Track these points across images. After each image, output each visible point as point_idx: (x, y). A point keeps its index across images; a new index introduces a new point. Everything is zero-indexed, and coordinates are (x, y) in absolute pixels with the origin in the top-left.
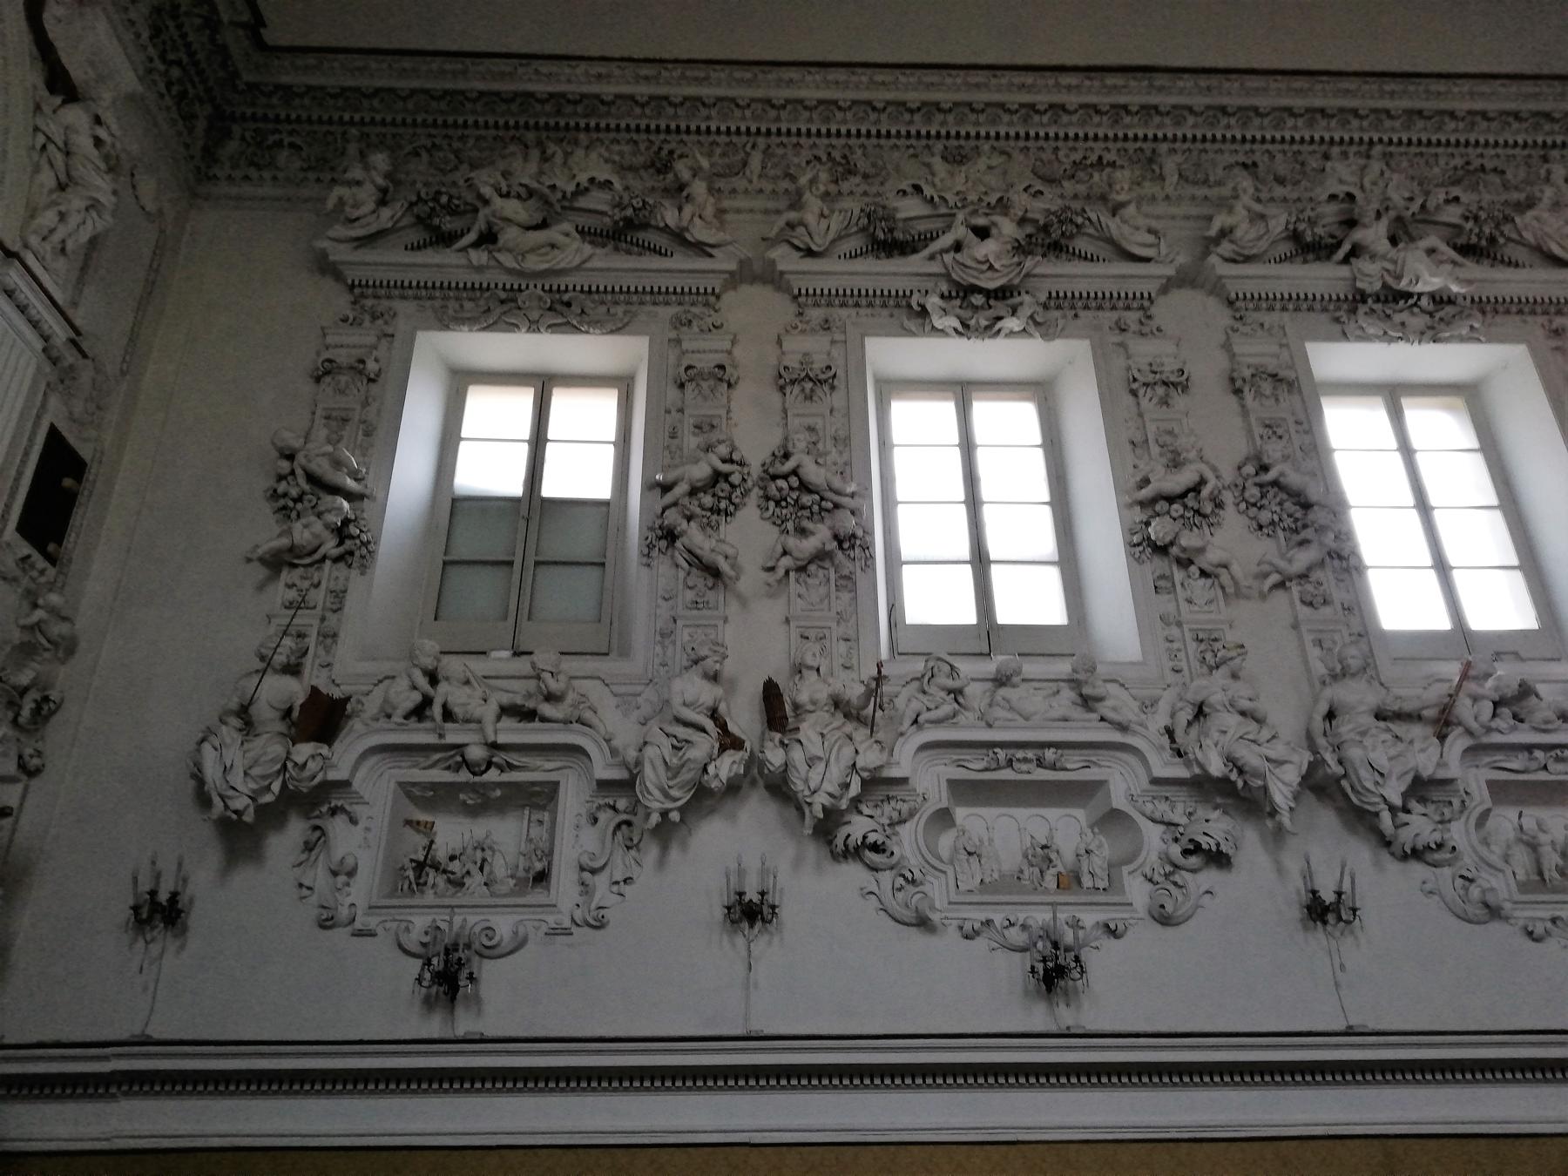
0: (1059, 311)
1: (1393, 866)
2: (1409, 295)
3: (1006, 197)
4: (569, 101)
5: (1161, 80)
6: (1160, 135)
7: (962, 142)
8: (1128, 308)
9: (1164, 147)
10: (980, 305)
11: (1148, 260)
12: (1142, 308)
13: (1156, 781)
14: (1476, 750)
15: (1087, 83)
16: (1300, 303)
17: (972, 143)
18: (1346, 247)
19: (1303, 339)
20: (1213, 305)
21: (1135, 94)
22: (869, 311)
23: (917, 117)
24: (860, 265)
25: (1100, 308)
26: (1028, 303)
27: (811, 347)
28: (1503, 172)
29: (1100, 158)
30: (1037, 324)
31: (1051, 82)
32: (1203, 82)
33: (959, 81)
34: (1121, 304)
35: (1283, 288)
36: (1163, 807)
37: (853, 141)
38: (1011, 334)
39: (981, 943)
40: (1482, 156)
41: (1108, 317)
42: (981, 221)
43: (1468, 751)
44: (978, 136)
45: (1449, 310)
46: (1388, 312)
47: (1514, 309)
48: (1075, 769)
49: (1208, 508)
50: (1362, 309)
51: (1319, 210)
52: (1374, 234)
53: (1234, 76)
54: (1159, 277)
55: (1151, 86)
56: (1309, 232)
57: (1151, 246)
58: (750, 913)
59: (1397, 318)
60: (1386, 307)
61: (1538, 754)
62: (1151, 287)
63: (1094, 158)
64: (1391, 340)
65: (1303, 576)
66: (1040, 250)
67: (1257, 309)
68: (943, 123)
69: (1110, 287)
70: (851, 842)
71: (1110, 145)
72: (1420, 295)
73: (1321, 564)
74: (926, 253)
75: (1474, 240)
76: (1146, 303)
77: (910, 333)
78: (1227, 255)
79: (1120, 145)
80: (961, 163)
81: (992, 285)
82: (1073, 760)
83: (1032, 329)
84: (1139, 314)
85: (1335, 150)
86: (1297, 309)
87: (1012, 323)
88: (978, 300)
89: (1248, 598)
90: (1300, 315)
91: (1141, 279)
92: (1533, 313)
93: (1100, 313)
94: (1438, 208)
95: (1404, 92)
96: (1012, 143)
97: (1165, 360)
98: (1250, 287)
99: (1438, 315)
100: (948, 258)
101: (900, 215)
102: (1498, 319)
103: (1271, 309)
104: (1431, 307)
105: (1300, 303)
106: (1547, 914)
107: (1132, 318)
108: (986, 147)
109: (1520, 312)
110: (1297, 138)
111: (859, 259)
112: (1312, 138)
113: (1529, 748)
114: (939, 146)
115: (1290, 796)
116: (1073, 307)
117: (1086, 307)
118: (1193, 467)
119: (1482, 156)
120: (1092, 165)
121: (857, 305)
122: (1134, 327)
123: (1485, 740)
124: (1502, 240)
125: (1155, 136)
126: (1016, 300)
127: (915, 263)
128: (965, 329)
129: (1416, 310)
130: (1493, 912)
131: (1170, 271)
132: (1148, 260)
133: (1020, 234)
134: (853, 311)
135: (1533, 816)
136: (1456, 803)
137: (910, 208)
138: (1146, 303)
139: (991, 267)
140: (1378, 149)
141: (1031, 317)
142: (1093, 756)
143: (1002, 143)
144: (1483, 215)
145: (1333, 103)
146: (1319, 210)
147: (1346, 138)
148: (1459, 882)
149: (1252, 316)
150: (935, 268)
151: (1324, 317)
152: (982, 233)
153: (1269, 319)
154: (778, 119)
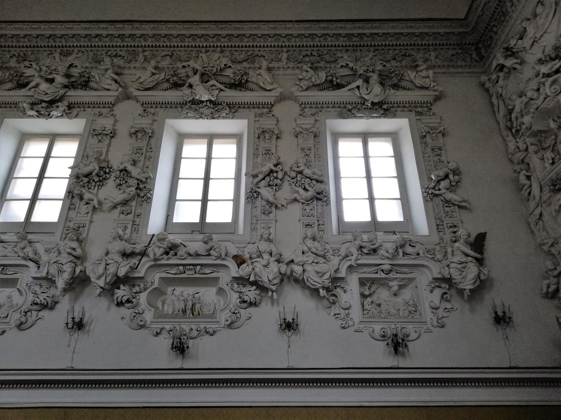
0: (71, 110)
1: (114, 308)
2: (202, 102)
3: (208, 67)
4: (150, 37)
5: (137, 25)
6: (140, 45)
7: (69, 49)
8: (104, 107)
9: (140, 49)
10: (45, 107)
11: (109, 90)
12: (109, 107)
13: (35, 278)
14: (156, 266)
15: (110, 27)
16: (166, 105)
17: (72, 49)
18: (187, 85)
19: (87, 119)
20: (138, 105)
21: (128, 30)
22: (10, 109)
23: (50, 40)
24: (13, 93)
25: (94, 107)
26: (62, 106)
27: (144, 122)
28: (264, 57)
29: (116, 54)
30: (66, 113)
31: (96, 26)
32: (152, 26)
33: (63, 27)
34: (101, 106)
35: (159, 100)
36: (37, 288)
37: (29, 49)
38: (57, 117)
39: (161, 337)
40: (259, 50)
41: (96, 110)
42: (50, 77)
43: (151, 267)
44: (73, 46)
45: (219, 106)
46: (197, 108)
47: (246, 106)
48: (10, 274)
49: (96, 179)
50: (187, 106)
51: (179, 71)
52: (195, 80)
53: (163, 23)
54: (114, 96)
55: (133, 27)
56: (171, 79)
57: (110, 85)
58: (79, 325)
59: (201, 110)
60: (194, 107)
61: (181, 268)
62: (112, 100)
63: (114, 54)
64: (197, 118)
65: (125, 203)
66: (80, 87)
67: (151, 107)
68: (295, 41)
69: (96, 100)
70: (119, 300)
71: (122, 49)
72: (207, 101)
73: (132, 199)
74: (28, 88)
75: (233, 81)
76: (111, 106)
77: (20, 117)
78: (136, 87)
79: (126, 49)
80: (67, 56)
81: (47, 99)
82: (10, 271)
83: (64, 114)
84: (109, 109)
85: (203, 50)
86: (166, 107)
87: (54, 113)
88: (44, 105)
89: (104, 211)
90: (167, 109)
91: (109, 96)
92: (254, 108)
93: (94, 109)
94: (221, 70)
95: (380, 26)
96: (87, 49)
97: (106, 126)
98: (148, 100)
99: (216, 109)
100: (33, 90)
101: (26, 75)
102: (240, 110)
103: (156, 107)
104: (212, 106)
105: (166, 105)
106: (161, 326)
107: (105, 111)
108: (76, 50)
109: (249, 108)
110: (190, 45)
111: (12, 91)
112: (195, 45)
113: (178, 265)
114: (59, 50)
115: (64, 284)
116: (84, 107)
117: (89, 107)
118: (92, 164)
119: (259, 50)
120: (114, 56)
121: (6, 107)
122: (104, 114)
123: (158, 262)
124: (243, 81)
125: (138, 45)
126: (56, 105)
127: (23, 92)
128: (40, 115)
129: (207, 107)
130: (142, 327)
131: (116, 94)
132: (109, 90)
133: (65, 81)
134: (4, 109)
135: (179, 290)
136: (142, 285)
137: (29, 72)
138: (111, 106)
139: (47, 93)
140: (219, 49)
141: (65, 110)
142: (17, 269)
143: (83, 49)
144: (238, 72)
145: (200, 32)
146: (179, 71)
147: (208, 45)
148: (135, 314)
149: (149, 110)
150: (30, 93)
151: (175, 110)
152: (51, 81)
153: (153, 110)
154: (37, 42)
